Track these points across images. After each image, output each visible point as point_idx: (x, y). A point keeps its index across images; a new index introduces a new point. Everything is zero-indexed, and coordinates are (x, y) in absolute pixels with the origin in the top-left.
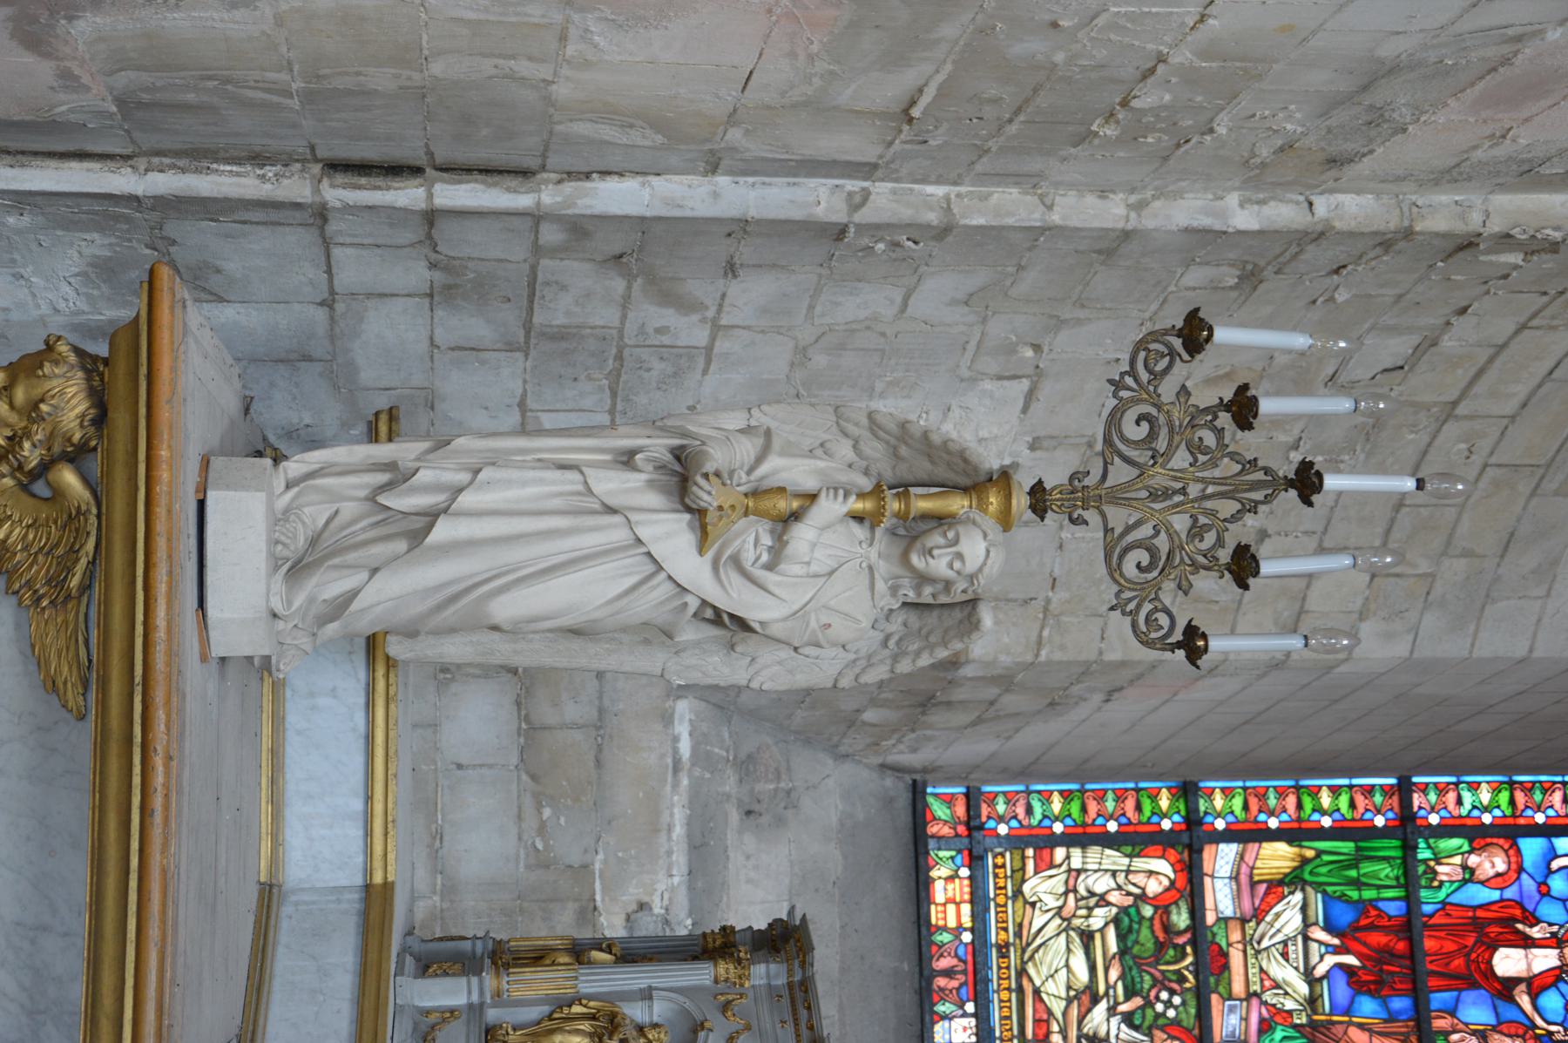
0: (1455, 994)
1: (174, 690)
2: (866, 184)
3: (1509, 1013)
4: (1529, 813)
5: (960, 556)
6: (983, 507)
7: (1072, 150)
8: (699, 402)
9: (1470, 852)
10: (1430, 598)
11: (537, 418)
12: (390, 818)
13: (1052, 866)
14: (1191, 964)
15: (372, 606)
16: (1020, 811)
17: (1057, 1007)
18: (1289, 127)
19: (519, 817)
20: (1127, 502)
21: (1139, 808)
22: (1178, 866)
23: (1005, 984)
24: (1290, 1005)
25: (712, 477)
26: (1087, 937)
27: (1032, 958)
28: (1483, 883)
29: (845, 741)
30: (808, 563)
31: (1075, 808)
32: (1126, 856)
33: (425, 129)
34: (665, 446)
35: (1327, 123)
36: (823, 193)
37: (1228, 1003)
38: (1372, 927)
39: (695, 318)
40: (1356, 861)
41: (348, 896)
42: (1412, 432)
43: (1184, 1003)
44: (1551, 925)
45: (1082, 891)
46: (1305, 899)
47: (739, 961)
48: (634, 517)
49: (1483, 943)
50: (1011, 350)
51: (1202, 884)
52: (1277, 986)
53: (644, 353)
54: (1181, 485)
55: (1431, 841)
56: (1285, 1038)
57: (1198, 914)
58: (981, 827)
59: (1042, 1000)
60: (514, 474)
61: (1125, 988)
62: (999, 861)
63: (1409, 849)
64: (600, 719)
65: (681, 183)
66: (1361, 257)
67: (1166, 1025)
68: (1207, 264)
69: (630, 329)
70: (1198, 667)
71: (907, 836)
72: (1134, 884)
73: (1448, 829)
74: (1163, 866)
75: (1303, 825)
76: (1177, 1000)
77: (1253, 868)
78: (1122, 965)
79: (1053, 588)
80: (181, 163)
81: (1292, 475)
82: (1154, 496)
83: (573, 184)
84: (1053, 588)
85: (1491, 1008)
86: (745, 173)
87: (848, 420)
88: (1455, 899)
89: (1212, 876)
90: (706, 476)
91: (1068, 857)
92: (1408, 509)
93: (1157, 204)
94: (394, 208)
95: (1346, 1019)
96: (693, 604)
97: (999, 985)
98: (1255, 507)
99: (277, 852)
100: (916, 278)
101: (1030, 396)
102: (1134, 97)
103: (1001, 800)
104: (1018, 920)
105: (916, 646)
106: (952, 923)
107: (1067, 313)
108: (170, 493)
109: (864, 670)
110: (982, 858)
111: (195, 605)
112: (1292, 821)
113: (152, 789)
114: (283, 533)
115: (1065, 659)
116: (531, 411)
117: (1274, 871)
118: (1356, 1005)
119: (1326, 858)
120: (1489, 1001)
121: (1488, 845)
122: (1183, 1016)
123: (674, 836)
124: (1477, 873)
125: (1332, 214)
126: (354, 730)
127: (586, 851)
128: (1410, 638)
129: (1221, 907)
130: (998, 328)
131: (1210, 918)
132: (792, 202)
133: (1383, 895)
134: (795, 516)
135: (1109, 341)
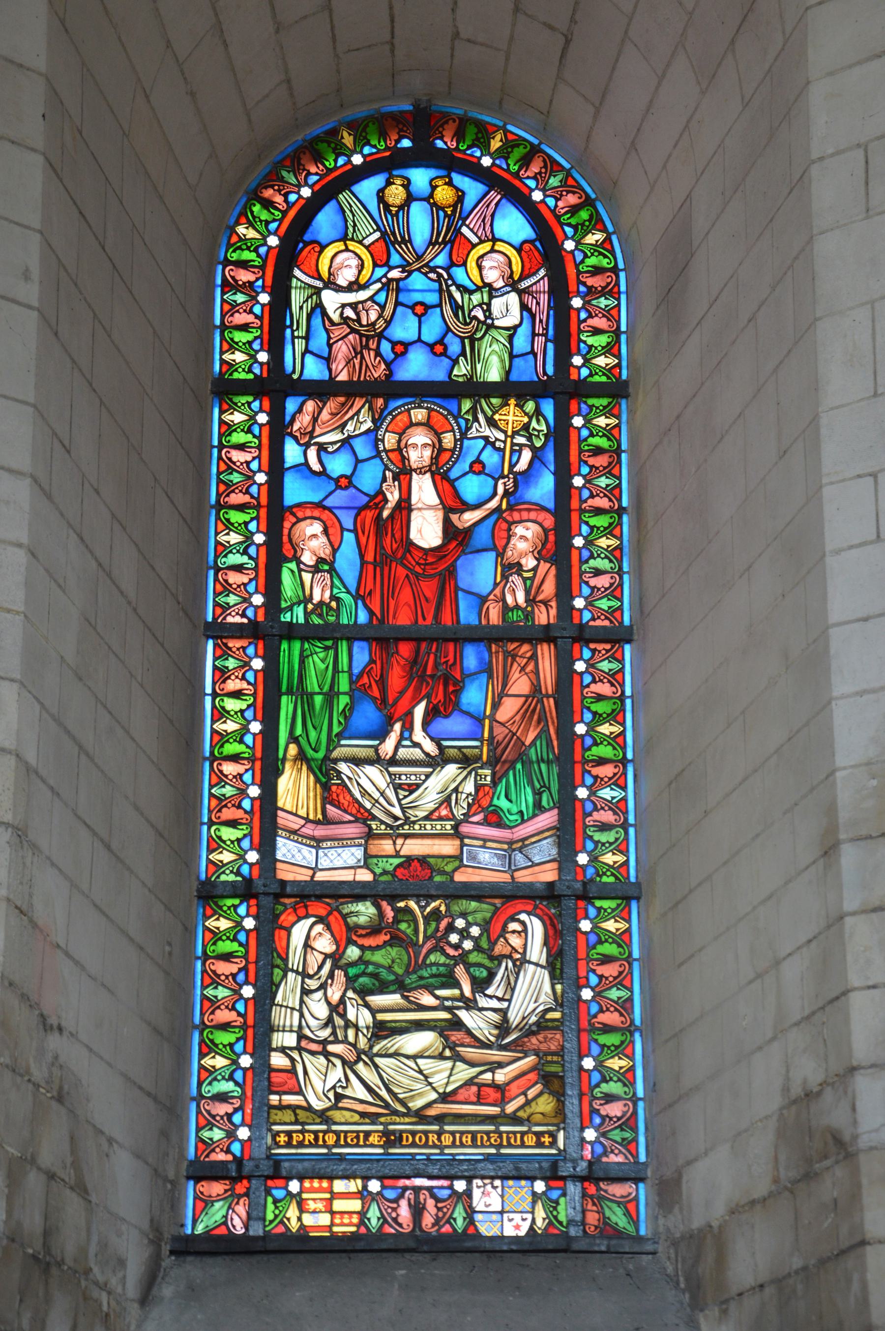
0: (461, 594)
3: (482, 536)
4: (254, 490)
9: (299, 562)
13: (293, 1071)
14: (417, 903)
16: (222, 1109)
17: (464, 1073)
21: (227, 957)
22: (301, 912)
23: (433, 1138)
24: (469, 787)
27: (402, 1102)
28: (335, 551)
31: (224, 1038)
32: (285, 976)
37: (465, 862)
38: (382, 683)
40: (303, 695)
43: (464, 915)
44: (384, 479)
45: (325, 1033)
46: (346, 760)
49: (404, 557)
52: (448, 800)
55: (284, 605)
56: (507, 796)
57: (357, 891)
58: (238, 1161)
59: (455, 1092)
61: (443, 986)
62: (282, 1139)
63: (291, 632)
67: (489, 938)
71: (242, 1263)
72: (320, 968)
73: (273, 589)
75: (259, 754)
76: (460, 923)
77: (307, 820)
78: (415, 989)
85: (476, 555)
88: (352, 584)
89: (315, 870)
91: (283, 1050)
95: (487, 721)
97: (434, 1146)
103: (206, 1134)
104: (356, 1117)
106: (356, 1205)
110: (277, 1163)
112: (252, 768)
117: (312, 794)
118: (472, 710)
119: (299, 731)
120: (470, 556)
121: (290, 540)
122: (479, 917)
124: (323, 556)
129: (352, 862)
131: (365, 876)
133: (346, 669)
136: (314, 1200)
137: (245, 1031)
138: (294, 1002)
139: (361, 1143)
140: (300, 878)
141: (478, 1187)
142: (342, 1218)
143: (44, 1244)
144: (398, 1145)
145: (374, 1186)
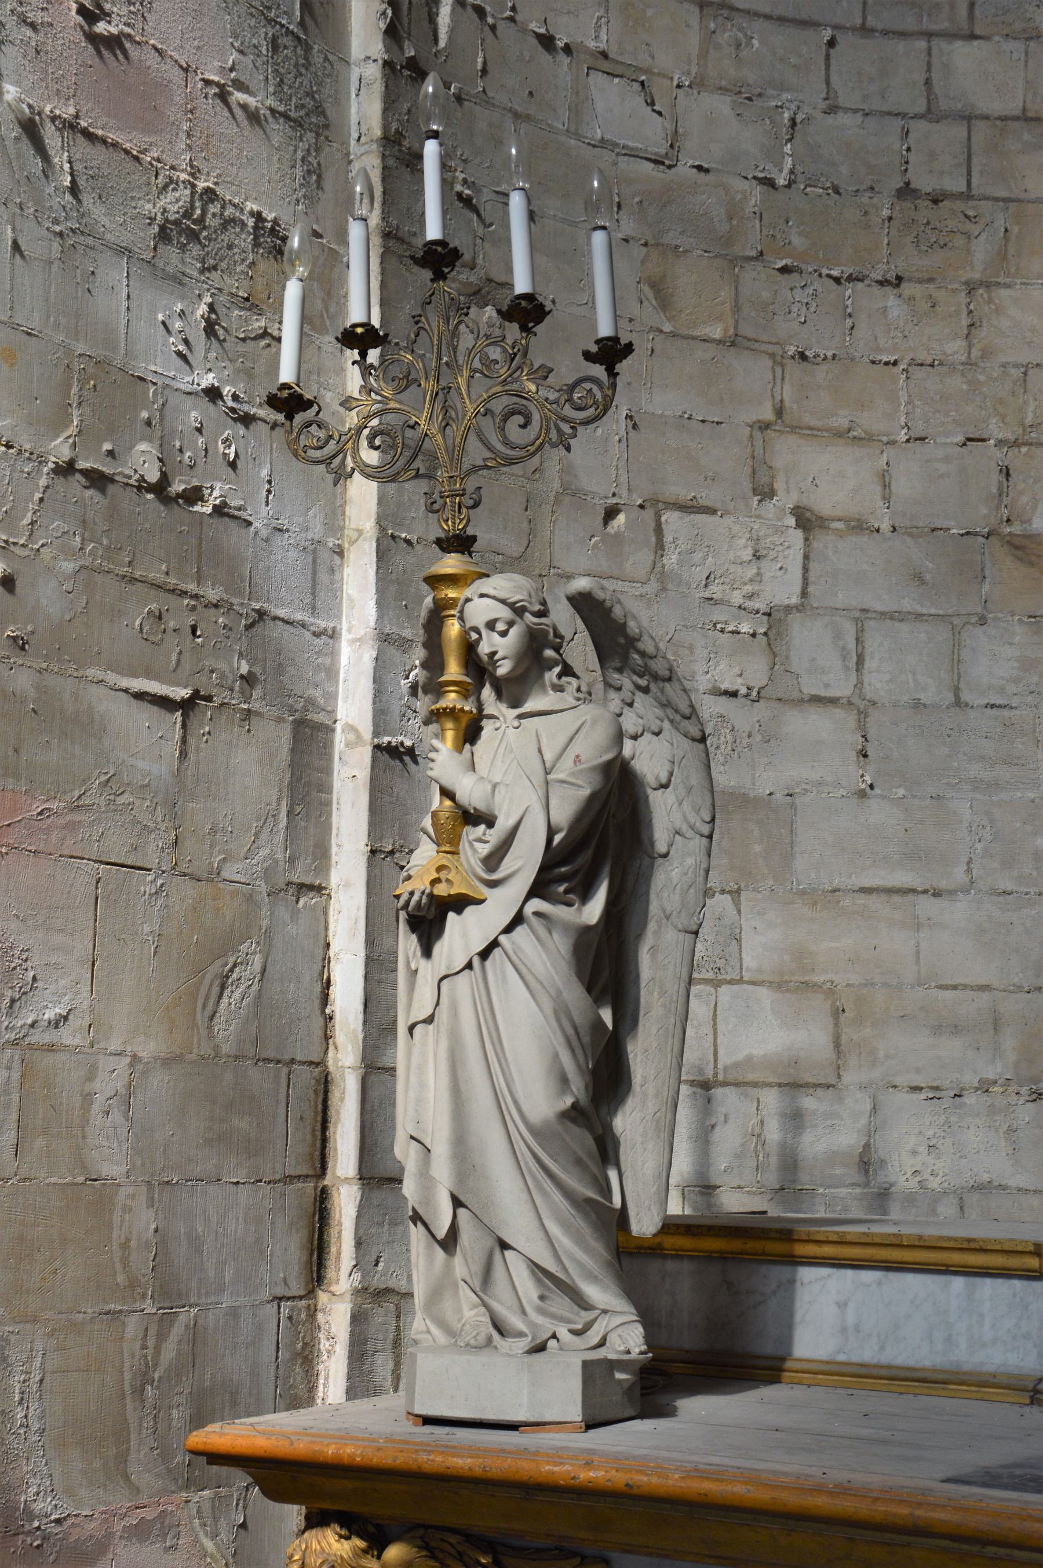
5: (491, 625)
12: (965, 1245)
65: (337, 921)
83: (337, 1033)
105: (636, 656)
109: (676, 711)
113: (609, 1484)
116: (716, 1074)
126: (880, 1284)
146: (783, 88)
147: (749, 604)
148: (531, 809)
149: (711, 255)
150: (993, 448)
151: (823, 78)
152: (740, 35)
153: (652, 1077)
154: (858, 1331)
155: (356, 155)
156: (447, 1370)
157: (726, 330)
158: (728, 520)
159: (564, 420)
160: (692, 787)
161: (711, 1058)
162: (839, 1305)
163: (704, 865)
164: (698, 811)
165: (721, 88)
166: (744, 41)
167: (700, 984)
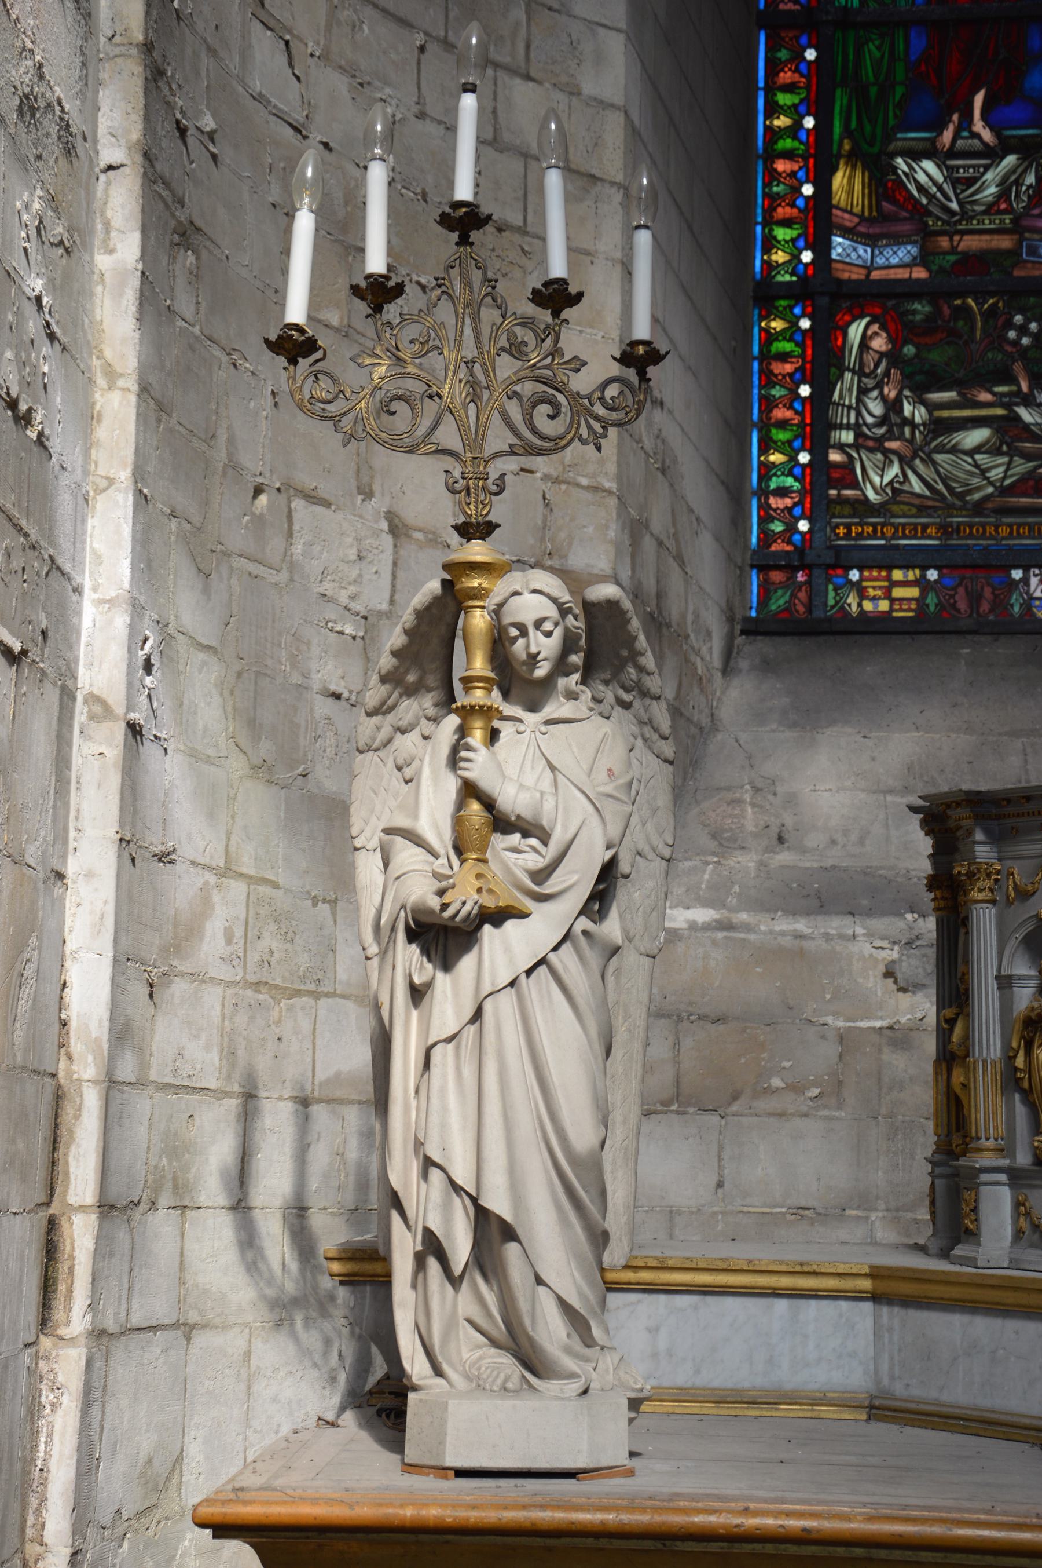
1: (671, 1505)
2: (80, 698)
5: (538, 624)
6: (480, 594)
7: (54, 459)
8: (308, 893)
10: (556, 6)
11: (321, 1084)
12: (798, 1269)
15: (575, 1282)
17: (1021, 467)
18: (36, 206)
19: (781, 1115)
20: (482, 427)
25: (446, 899)
26: (939, 427)
29: (695, 719)
30: (542, 793)
32: (841, 376)
33: (15, 1214)
34: (405, 949)
35: (32, 160)
36: (91, 748)
39: (216, 897)
41: (885, 1319)
42: (361, 28)
43: (1022, 311)
47: (970, 875)
48: (487, 989)
50: (259, 520)
51: (880, 282)
53: (254, 957)
54: (463, 365)
59: (1012, 486)
60: (434, 1119)
62: (841, 531)
64: (669, 1016)
65: (74, 915)
66: (168, 103)
68: (172, 289)
69: (224, 973)
70: (667, 353)
74: (855, 331)
76: (1018, 319)
79: (531, 472)
80: (34, 1502)
81: (455, 236)
82: (475, 398)
83: (72, 1042)
84: (531, 472)
86: (65, 841)
87: (374, 740)
90: (445, 907)
91: (841, 447)
92: (450, 33)
93: (108, 353)
94: (96, 1250)
96: (584, 923)
97: (991, 537)
98: (490, 281)
99: (833, 1399)
100: (180, 638)
101: (312, 498)
102: (8, 394)
104: (914, 511)
105: (632, 670)
106: (914, 592)
107: (220, 456)
108: (454, 1507)
111: (573, 1481)
113: (781, 1530)
114: (494, 1381)
115: (615, 458)
119: (854, 124)
123: (807, 931)
125: (123, 142)
126: (696, 1308)
127: (823, 1037)
128: (601, 31)
130: (237, 538)
131: (920, 273)
132: (99, 786)
133: (902, 56)
134: (489, 804)
135: (252, 404)
136: (874, 588)
137: (804, 429)
138: (850, 400)
139: (919, 534)
140: (854, 277)
141: (1035, 575)
142: (900, 605)
143: (657, 605)
144: (955, 536)
145: (932, 575)
146: (387, 83)
147: (353, 605)
148: (587, 822)
149: (332, 238)
150: (539, 481)
151: (415, 81)
152: (355, 17)
153: (619, 1104)
154: (671, 1356)
155: (107, 54)
156: (487, 1417)
157: (342, 319)
158: (340, 516)
159: (597, 418)
160: (658, 808)
161: (310, 1075)
162: (649, 1330)
163: (664, 889)
164: (661, 834)
165: (340, 67)
166: (358, 23)
167: (305, 996)
